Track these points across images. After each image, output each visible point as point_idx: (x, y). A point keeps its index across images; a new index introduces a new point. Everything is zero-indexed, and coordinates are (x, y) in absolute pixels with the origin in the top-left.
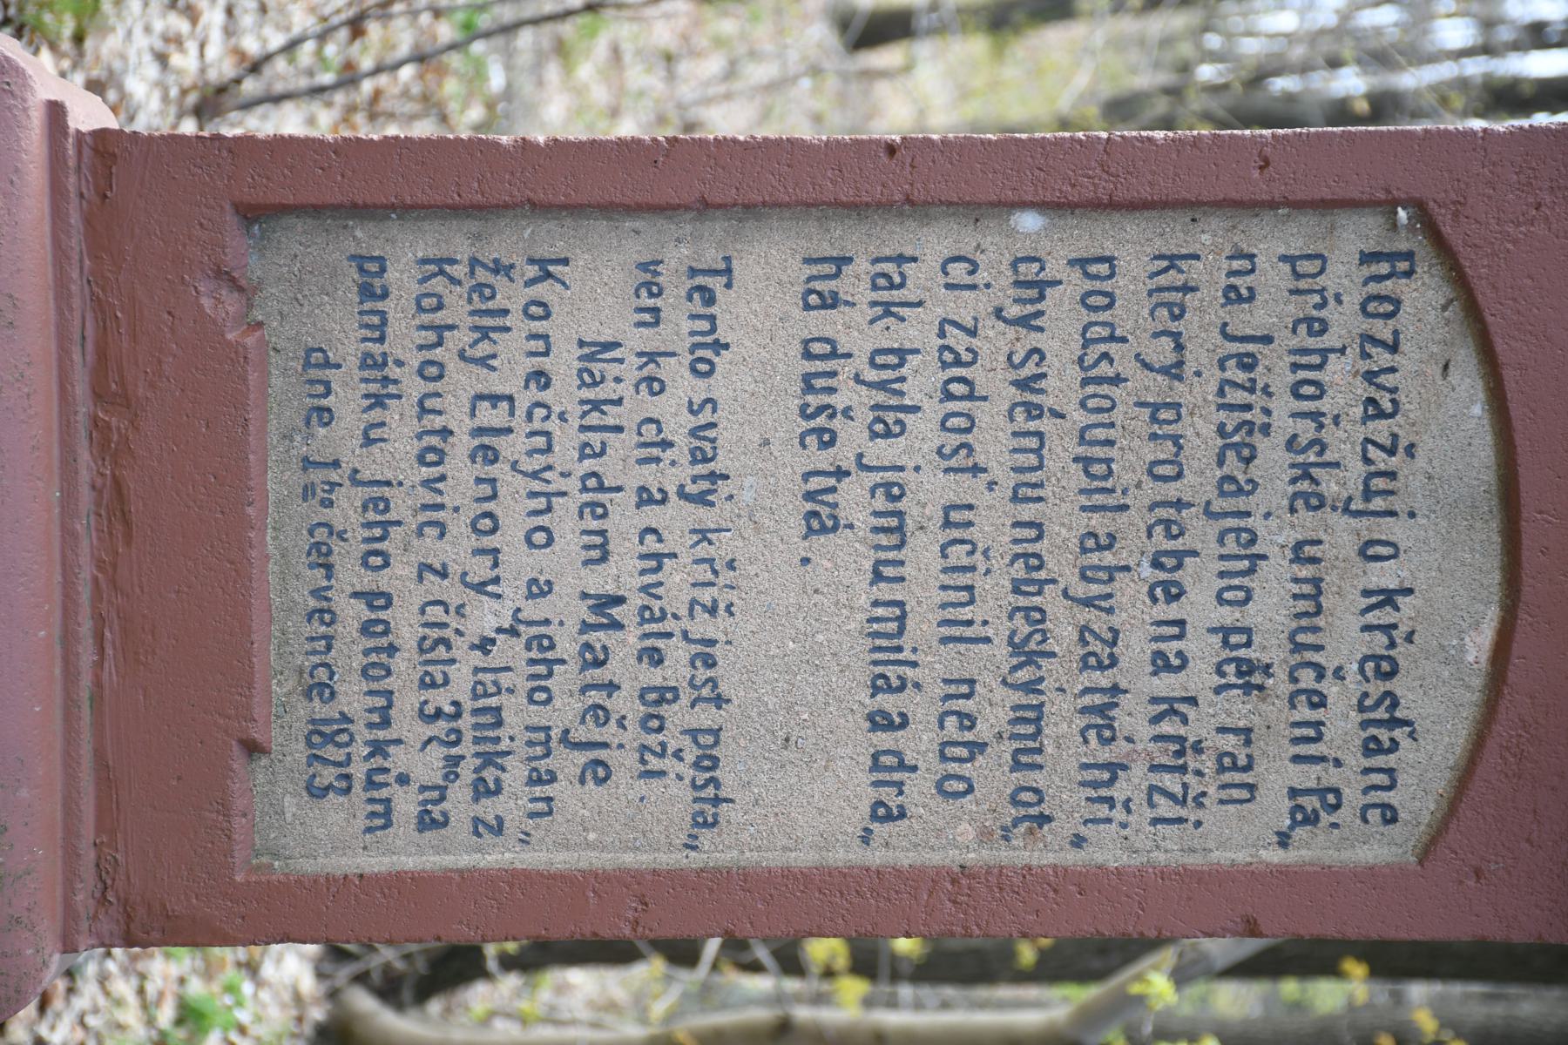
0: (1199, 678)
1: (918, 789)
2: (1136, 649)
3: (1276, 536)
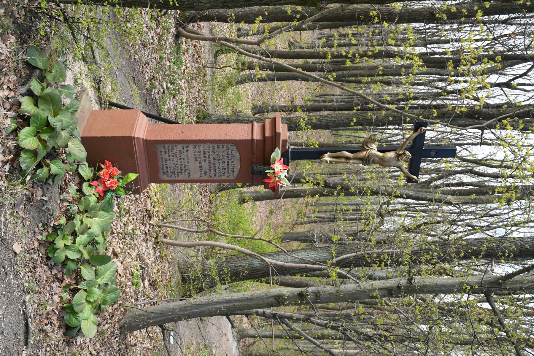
0: (221, 169)
1: (203, 175)
2: (217, 167)
3: (226, 161)
